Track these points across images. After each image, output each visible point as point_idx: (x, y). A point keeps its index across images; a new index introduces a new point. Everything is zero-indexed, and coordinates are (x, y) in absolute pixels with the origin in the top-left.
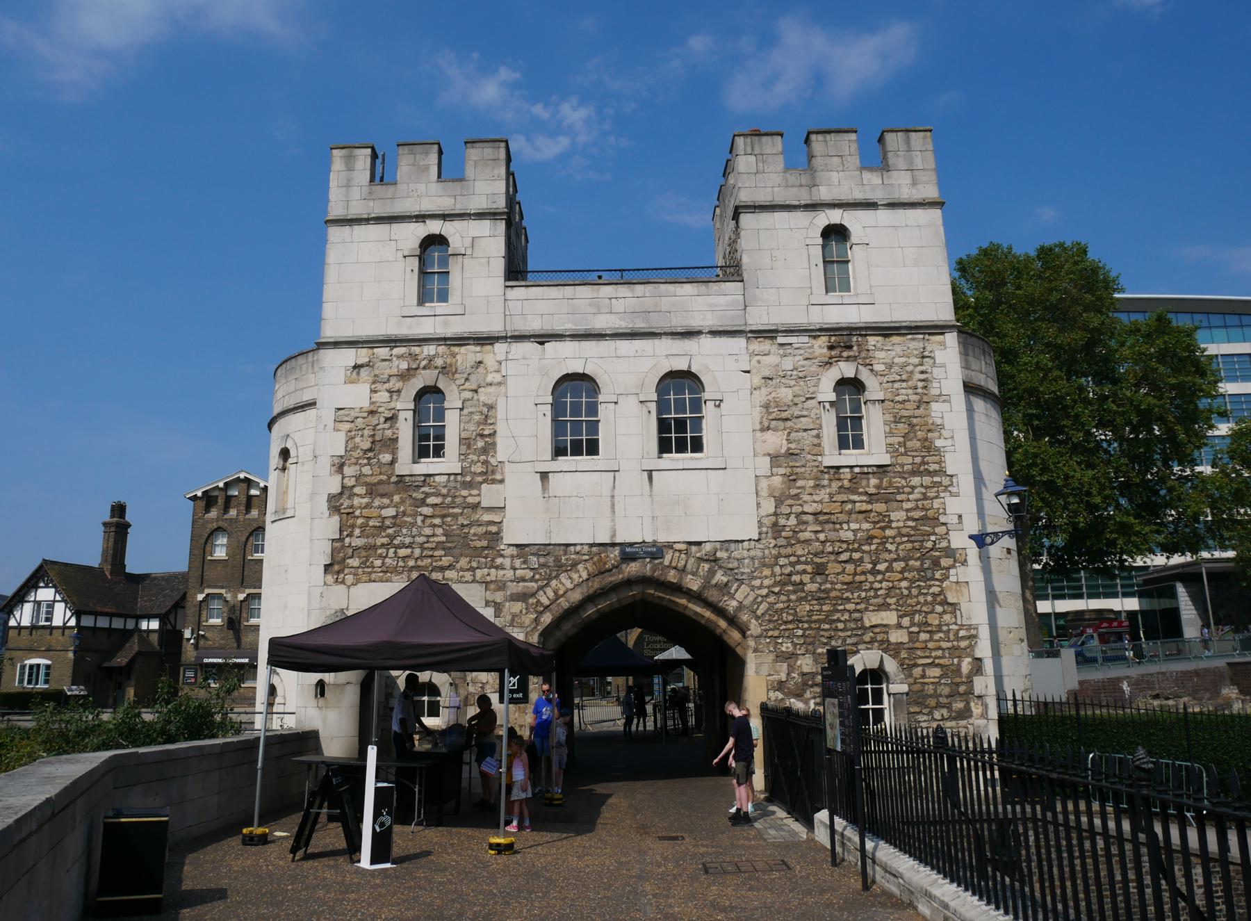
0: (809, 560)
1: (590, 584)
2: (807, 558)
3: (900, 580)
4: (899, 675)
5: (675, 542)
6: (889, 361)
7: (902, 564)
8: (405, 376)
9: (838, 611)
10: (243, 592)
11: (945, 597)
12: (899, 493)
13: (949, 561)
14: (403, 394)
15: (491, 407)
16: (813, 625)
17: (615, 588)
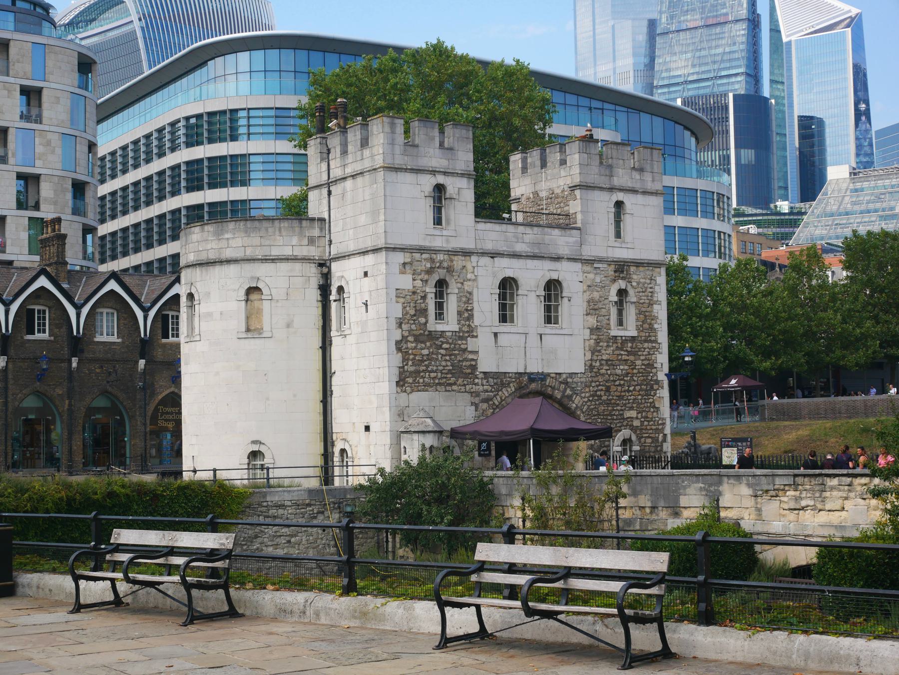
7: (639, 387)
8: (430, 272)
9: (614, 410)
15: (470, 293)
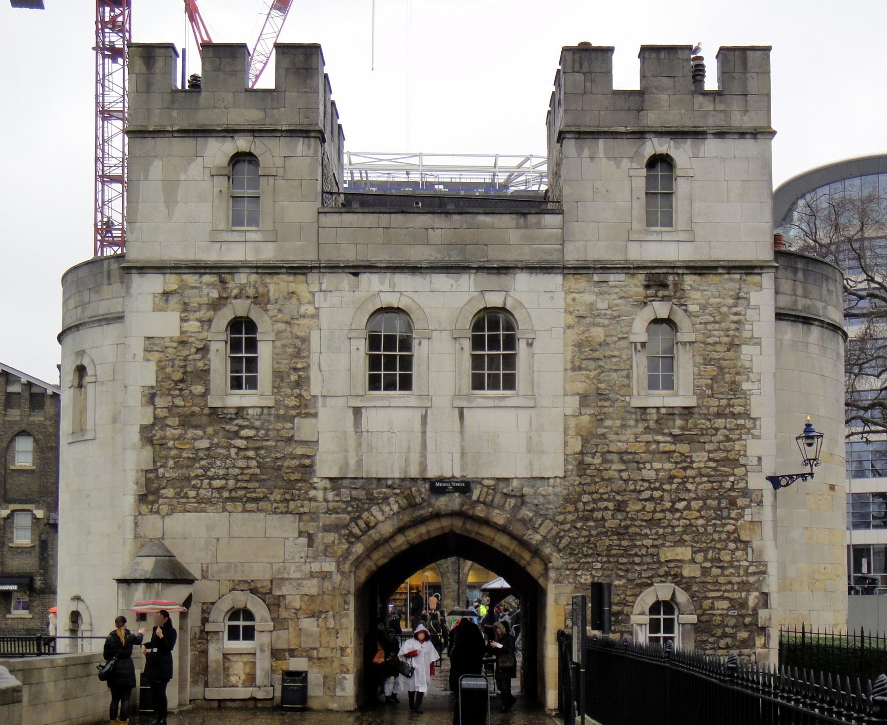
0: (611, 497)
1: (401, 517)
2: (609, 496)
3: (696, 519)
4: (689, 607)
5: (483, 478)
6: (704, 302)
7: (700, 503)
8: (216, 305)
9: (636, 546)
10: (7, 508)
11: (738, 534)
12: (702, 435)
13: (746, 501)
14: (214, 324)
15: (305, 340)
16: (611, 559)
17: (423, 520)
